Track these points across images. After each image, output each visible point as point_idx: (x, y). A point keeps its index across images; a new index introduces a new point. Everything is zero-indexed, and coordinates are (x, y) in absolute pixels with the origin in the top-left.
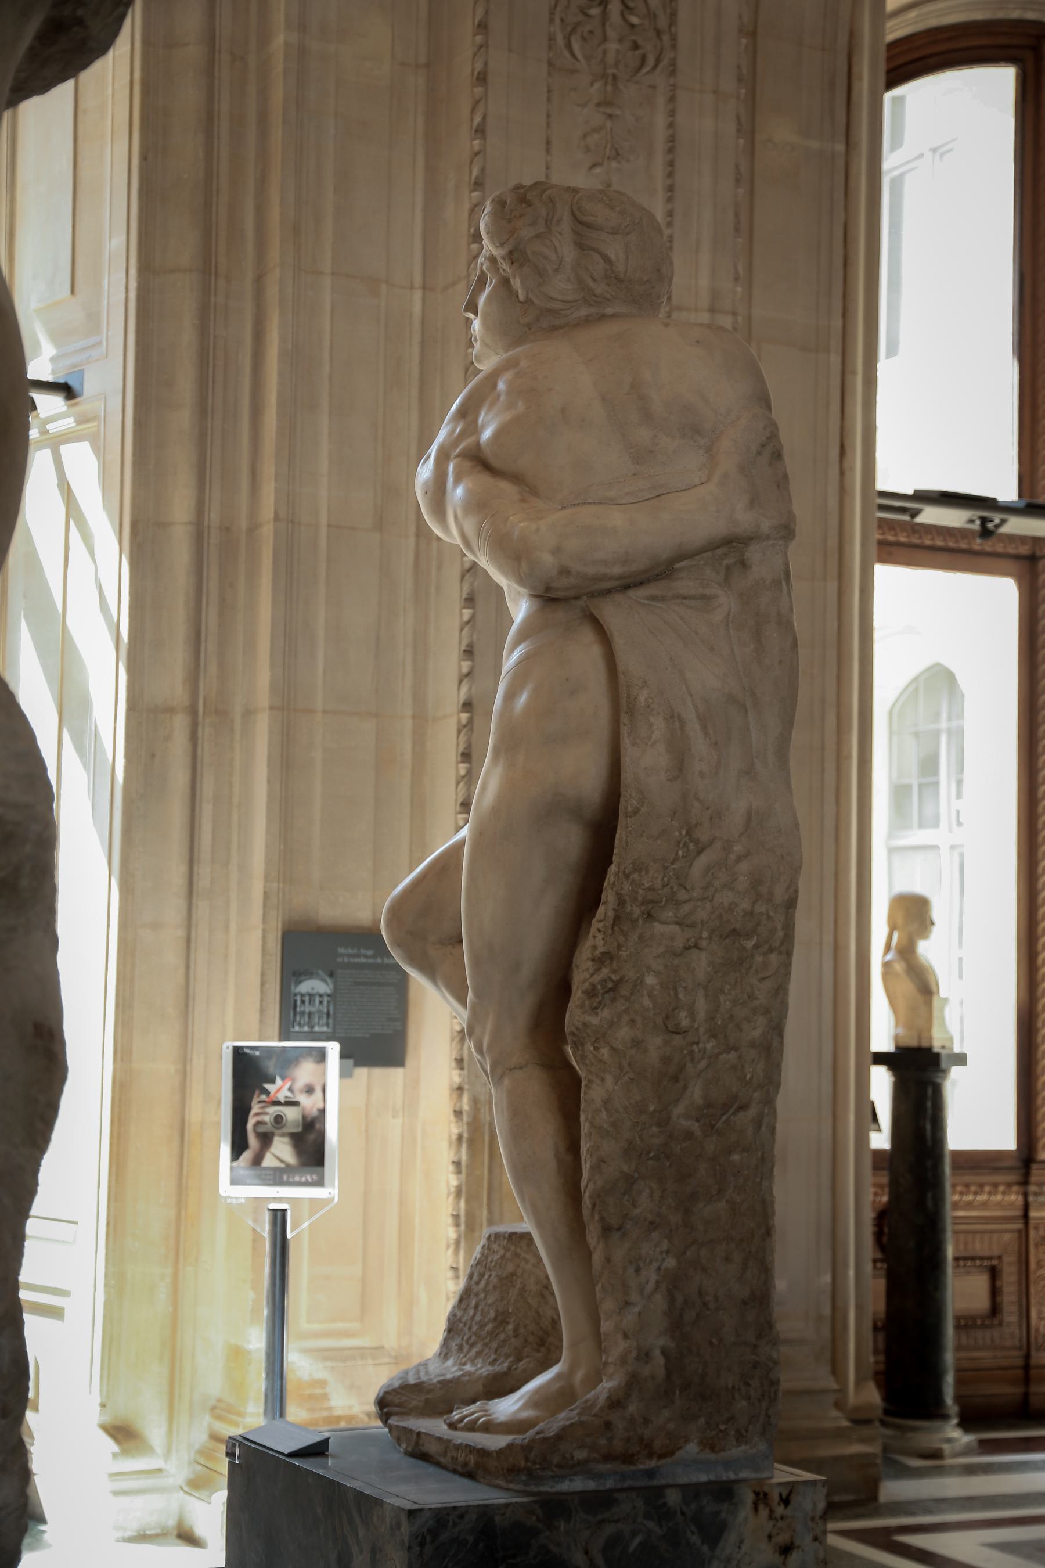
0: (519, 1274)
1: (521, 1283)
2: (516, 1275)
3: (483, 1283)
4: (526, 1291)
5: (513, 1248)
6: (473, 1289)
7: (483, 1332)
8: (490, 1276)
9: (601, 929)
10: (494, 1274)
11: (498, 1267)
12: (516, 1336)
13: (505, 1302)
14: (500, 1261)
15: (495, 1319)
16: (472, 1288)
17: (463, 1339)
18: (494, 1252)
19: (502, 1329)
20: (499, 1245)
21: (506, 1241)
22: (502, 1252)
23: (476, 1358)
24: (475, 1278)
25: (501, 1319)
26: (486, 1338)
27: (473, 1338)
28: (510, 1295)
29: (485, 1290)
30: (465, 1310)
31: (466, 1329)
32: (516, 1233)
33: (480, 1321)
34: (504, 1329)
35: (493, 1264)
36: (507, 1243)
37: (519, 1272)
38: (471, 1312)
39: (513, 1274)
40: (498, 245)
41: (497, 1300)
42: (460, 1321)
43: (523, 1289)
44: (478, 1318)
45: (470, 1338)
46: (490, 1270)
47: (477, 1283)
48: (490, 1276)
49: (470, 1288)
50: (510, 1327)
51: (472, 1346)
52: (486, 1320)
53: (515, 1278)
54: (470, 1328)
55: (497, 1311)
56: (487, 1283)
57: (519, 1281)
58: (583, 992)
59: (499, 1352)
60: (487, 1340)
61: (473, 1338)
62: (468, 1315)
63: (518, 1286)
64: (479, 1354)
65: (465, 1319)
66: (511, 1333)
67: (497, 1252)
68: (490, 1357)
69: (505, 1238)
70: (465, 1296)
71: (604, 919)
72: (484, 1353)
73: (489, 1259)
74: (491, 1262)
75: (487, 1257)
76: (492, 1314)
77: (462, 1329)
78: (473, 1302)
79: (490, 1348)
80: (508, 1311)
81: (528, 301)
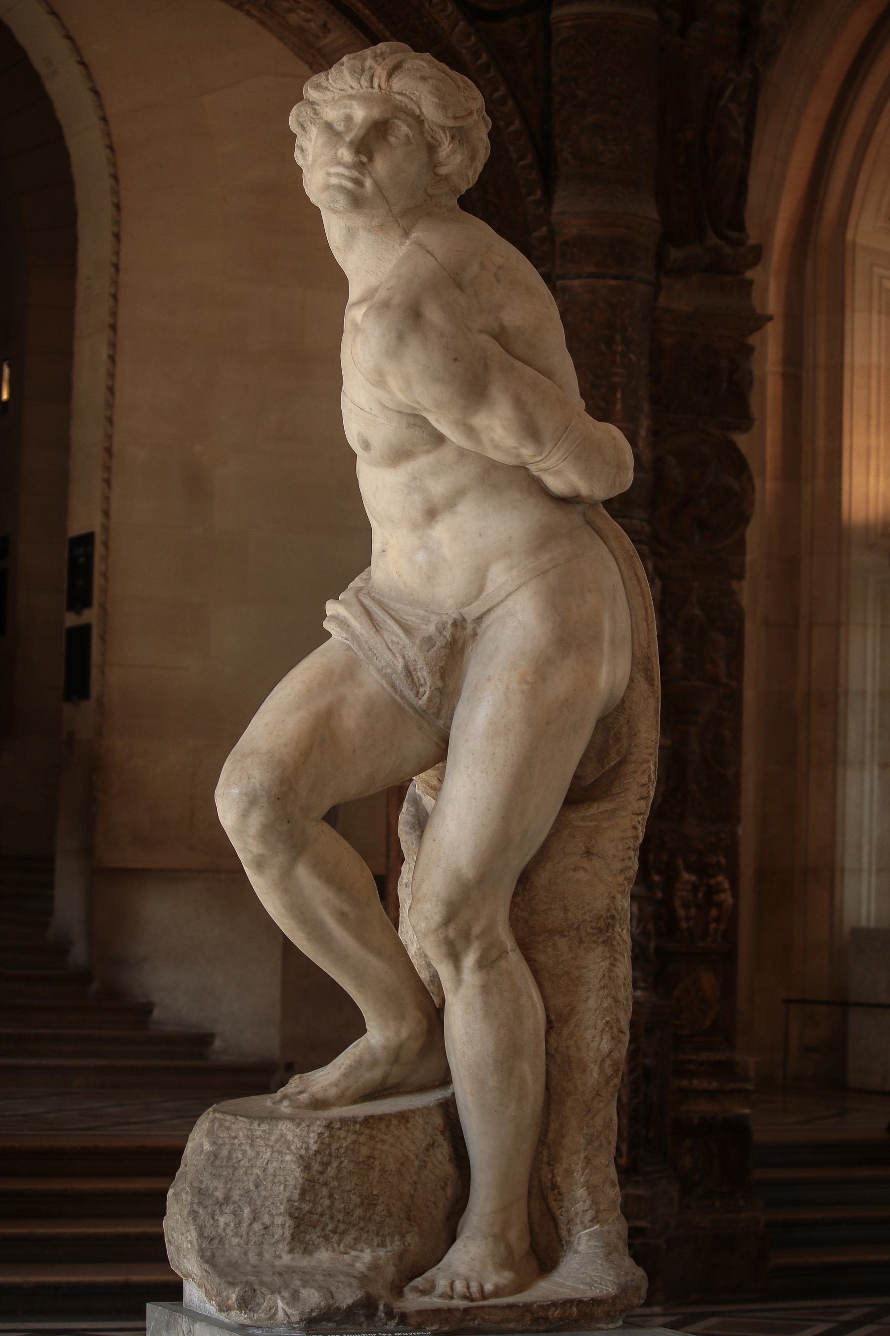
0: (376, 1156)
1: (380, 1164)
2: (374, 1158)
3: (331, 1171)
4: (387, 1171)
5: (368, 1131)
6: (318, 1179)
7: (353, 1219)
8: (341, 1163)
9: (641, 822)
10: (345, 1163)
11: (349, 1152)
12: (391, 1215)
13: (367, 1185)
14: (352, 1146)
15: (362, 1203)
16: (316, 1178)
17: (323, 1229)
18: (339, 1138)
19: (371, 1212)
20: (348, 1131)
21: (358, 1126)
22: (352, 1137)
23: (355, 1244)
24: (316, 1167)
25: (369, 1202)
26: (359, 1223)
27: (342, 1227)
28: (371, 1178)
29: (336, 1178)
30: (314, 1202)
31: (326, 1219)
32: (372, 1116)
33: (345, 1208)
34: (374, 1210)
35: (342, 1151)
36: (360, 1128)
37: (376, 1153)
38: (327, 1202)
39: (369, 1157)
40: (450, 115)
41: (356, 1184)
42: (310, 1212)
43: (383, 1171)
44: (339, 1205)
45: (337, 1227)
46: (337, 1157)
47: (322, 1173)
48: (341, 1163)
49: (314, 1178)
50: (380, 1208)
51: (343, 1234)
52: (351, 1206)
53: (372, 1160)
54: (332, 1218)
55: (361, 1196)
56: (339, 1169)
57: (377, 1163)
58: (626, 879)
59: (381, 1233)
60: (362, 1224)
61: (342, 1227)
62: (322, 1205)
63: (378, 1168)
64: (357, 1240)
65: (320, 1210)
66: (384, 1213)
67: (345, 1138)
68: (372, 1240)
69: (356, 1122)
70: (307, 1187)
71: (645, 813)
72: (363, 1238)
73: (334, 1147)
74: (337, 1149)
75: (329, 1145)
76: (355, 1199)
77: (318, 1221)
78: (325, 1192)
79: (368, 1232)
80: (372, 1192)
81: (447, 178)
